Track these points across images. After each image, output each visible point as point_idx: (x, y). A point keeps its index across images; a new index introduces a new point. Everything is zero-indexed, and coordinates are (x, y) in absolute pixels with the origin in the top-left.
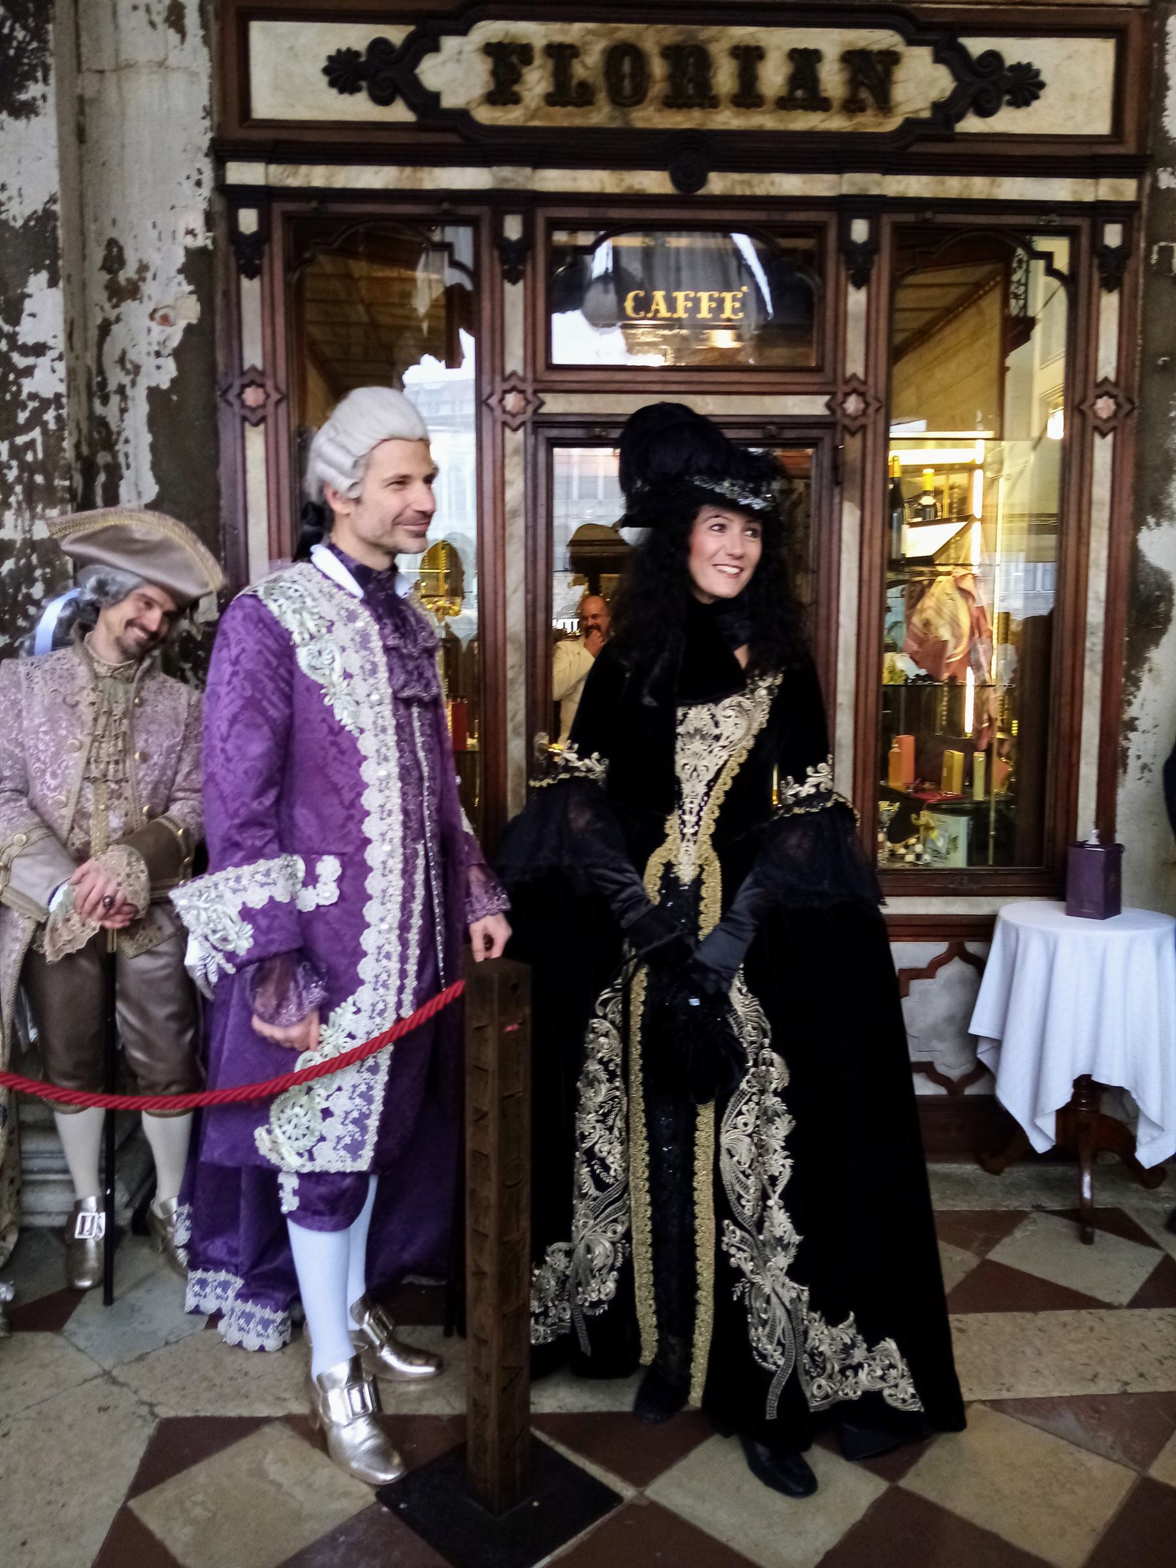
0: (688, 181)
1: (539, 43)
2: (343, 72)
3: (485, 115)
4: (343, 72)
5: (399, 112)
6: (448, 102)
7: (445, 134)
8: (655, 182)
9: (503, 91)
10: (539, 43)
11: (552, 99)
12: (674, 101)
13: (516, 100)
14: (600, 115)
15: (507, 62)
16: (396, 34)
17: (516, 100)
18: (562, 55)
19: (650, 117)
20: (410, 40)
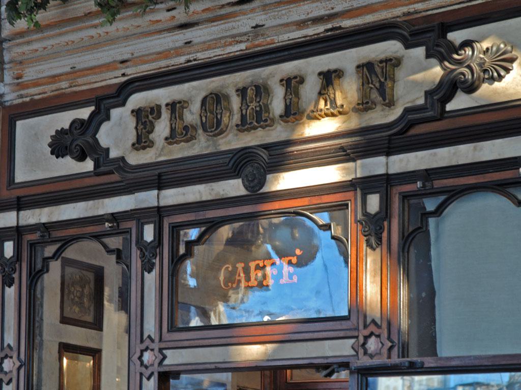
0: (255, 184)
1: (163, 103)
2: (61, 145)
3: (135, 159)
4: (61, 145)
5: (88, 165)
6: (113, 154)
7: (116, 177)
8: (234, 187)
9: (142, 142)
10: (163, 103)
11: (171, 139)
12: (244, 126)
13: (151, 144)
14: (200, 146)
15: (145, 119)
16: (84, 113)
17: (151, 144)
18: (175, 107)
19: (232, 141)
20: (93, 115)
